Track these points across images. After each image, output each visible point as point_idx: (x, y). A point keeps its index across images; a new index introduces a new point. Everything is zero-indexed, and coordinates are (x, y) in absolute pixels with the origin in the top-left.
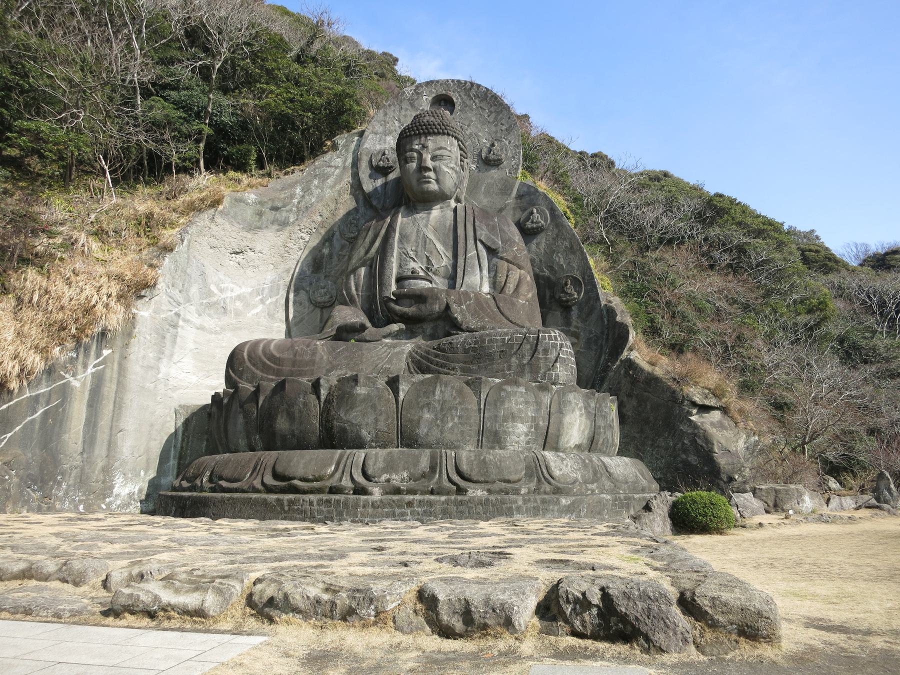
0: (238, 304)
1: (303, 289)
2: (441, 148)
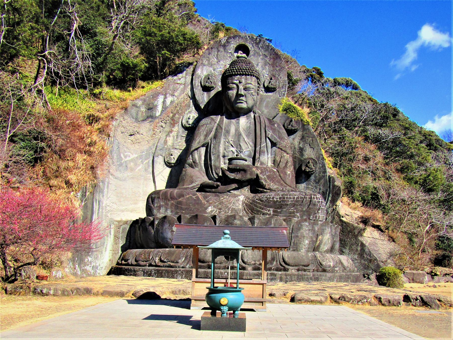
0: (132, 164)
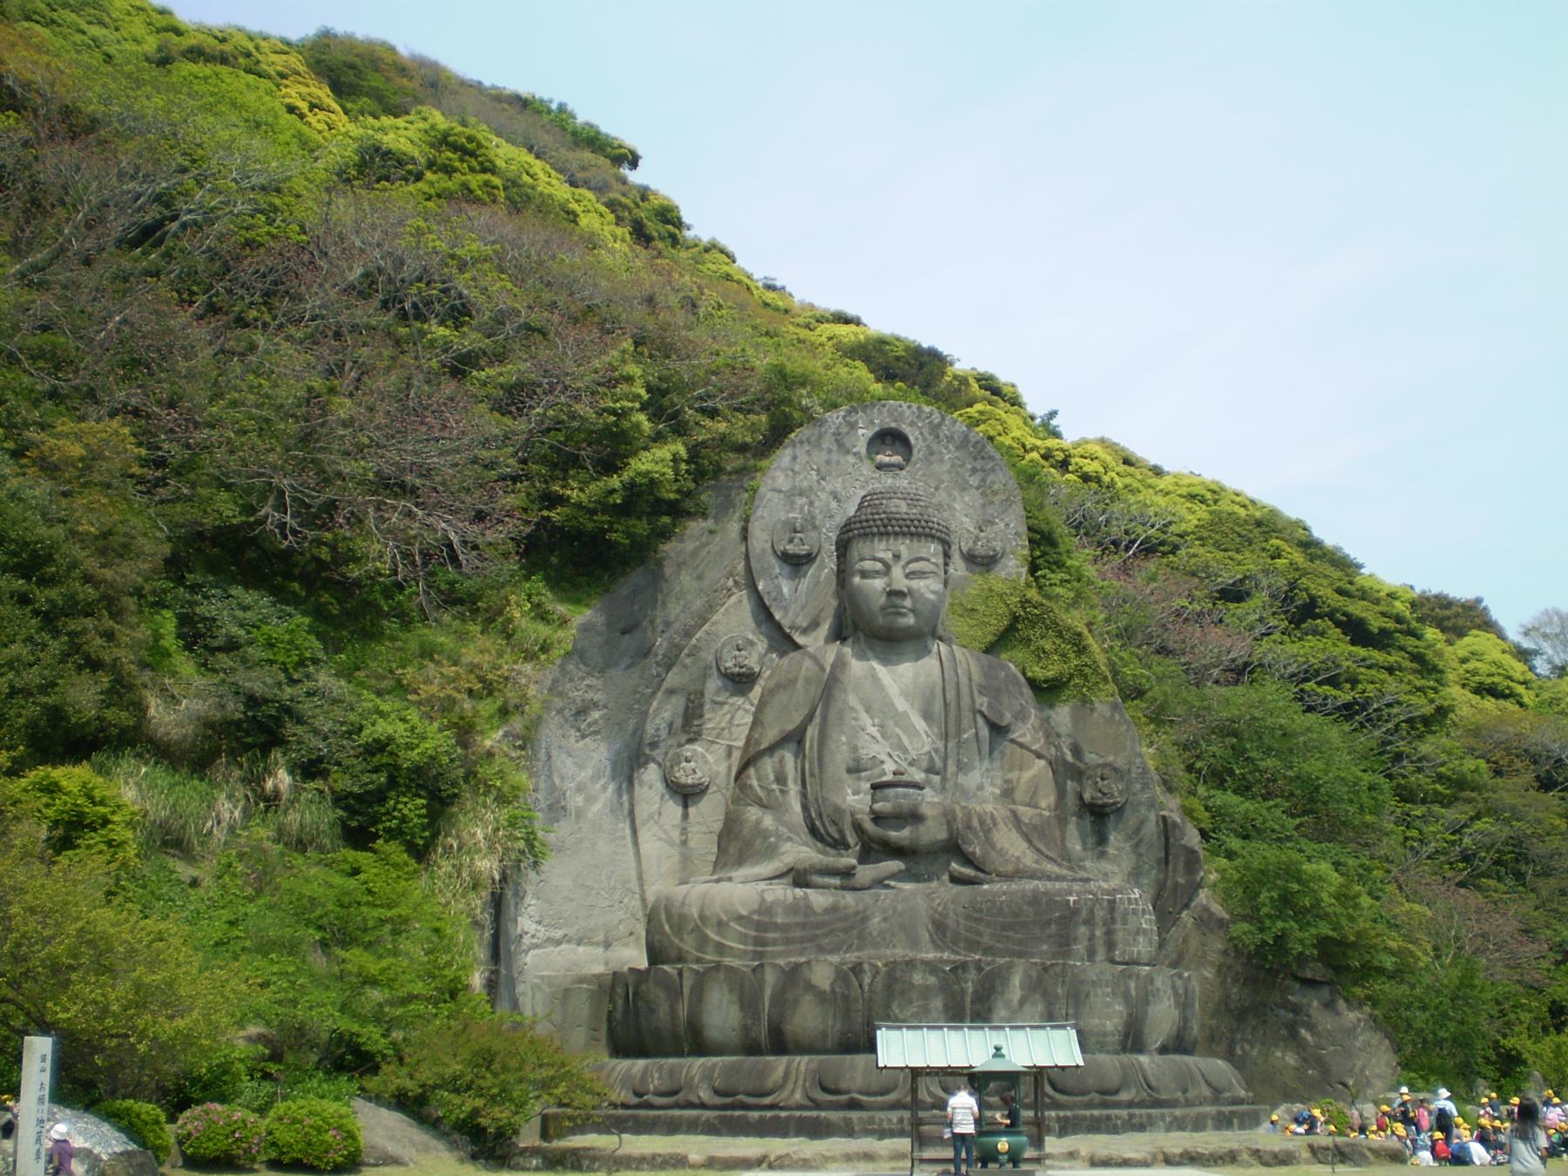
1: (654, 760)
2: (918, 560)
